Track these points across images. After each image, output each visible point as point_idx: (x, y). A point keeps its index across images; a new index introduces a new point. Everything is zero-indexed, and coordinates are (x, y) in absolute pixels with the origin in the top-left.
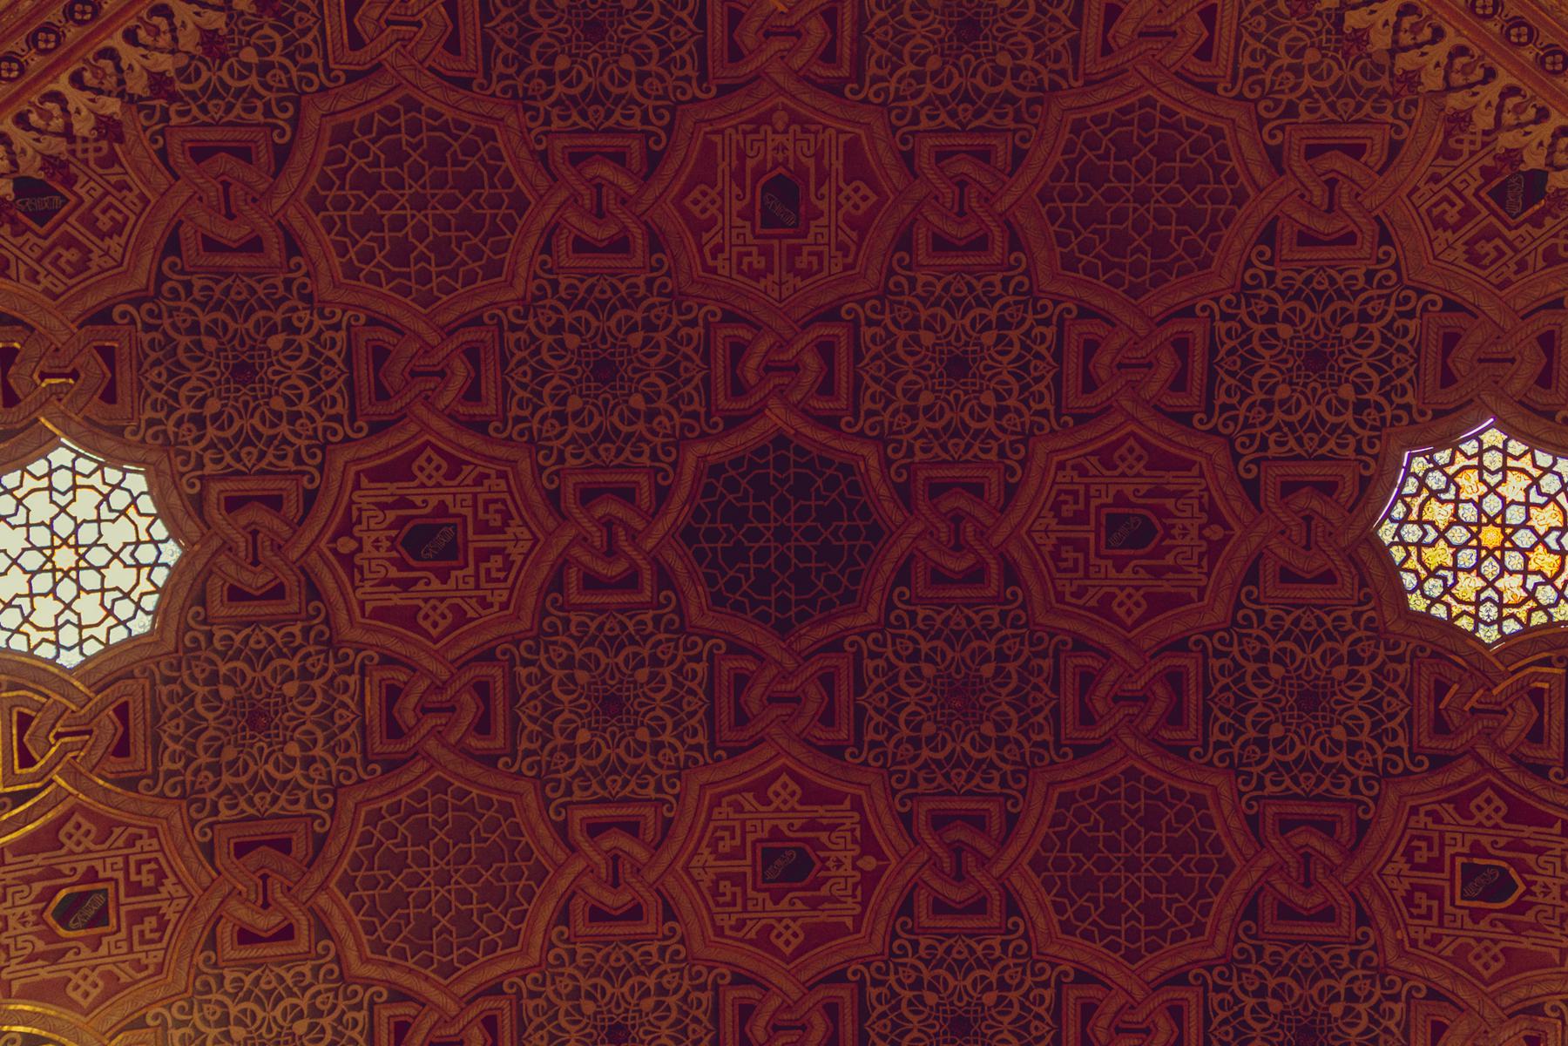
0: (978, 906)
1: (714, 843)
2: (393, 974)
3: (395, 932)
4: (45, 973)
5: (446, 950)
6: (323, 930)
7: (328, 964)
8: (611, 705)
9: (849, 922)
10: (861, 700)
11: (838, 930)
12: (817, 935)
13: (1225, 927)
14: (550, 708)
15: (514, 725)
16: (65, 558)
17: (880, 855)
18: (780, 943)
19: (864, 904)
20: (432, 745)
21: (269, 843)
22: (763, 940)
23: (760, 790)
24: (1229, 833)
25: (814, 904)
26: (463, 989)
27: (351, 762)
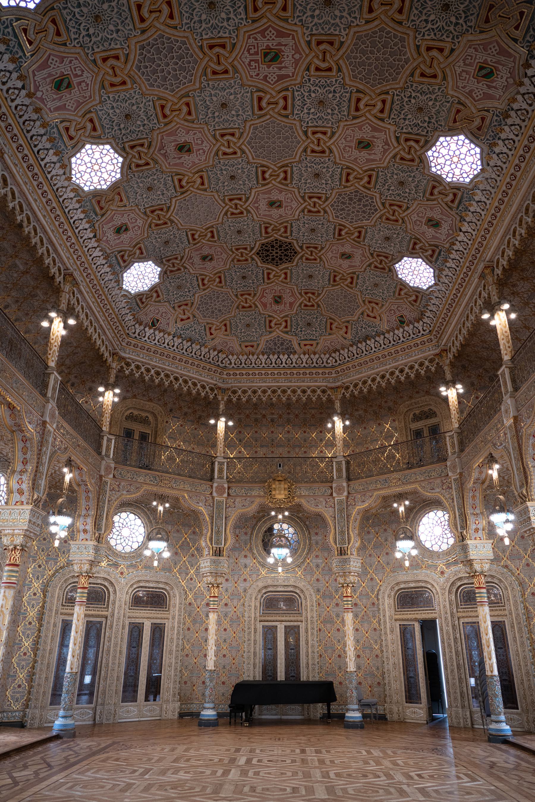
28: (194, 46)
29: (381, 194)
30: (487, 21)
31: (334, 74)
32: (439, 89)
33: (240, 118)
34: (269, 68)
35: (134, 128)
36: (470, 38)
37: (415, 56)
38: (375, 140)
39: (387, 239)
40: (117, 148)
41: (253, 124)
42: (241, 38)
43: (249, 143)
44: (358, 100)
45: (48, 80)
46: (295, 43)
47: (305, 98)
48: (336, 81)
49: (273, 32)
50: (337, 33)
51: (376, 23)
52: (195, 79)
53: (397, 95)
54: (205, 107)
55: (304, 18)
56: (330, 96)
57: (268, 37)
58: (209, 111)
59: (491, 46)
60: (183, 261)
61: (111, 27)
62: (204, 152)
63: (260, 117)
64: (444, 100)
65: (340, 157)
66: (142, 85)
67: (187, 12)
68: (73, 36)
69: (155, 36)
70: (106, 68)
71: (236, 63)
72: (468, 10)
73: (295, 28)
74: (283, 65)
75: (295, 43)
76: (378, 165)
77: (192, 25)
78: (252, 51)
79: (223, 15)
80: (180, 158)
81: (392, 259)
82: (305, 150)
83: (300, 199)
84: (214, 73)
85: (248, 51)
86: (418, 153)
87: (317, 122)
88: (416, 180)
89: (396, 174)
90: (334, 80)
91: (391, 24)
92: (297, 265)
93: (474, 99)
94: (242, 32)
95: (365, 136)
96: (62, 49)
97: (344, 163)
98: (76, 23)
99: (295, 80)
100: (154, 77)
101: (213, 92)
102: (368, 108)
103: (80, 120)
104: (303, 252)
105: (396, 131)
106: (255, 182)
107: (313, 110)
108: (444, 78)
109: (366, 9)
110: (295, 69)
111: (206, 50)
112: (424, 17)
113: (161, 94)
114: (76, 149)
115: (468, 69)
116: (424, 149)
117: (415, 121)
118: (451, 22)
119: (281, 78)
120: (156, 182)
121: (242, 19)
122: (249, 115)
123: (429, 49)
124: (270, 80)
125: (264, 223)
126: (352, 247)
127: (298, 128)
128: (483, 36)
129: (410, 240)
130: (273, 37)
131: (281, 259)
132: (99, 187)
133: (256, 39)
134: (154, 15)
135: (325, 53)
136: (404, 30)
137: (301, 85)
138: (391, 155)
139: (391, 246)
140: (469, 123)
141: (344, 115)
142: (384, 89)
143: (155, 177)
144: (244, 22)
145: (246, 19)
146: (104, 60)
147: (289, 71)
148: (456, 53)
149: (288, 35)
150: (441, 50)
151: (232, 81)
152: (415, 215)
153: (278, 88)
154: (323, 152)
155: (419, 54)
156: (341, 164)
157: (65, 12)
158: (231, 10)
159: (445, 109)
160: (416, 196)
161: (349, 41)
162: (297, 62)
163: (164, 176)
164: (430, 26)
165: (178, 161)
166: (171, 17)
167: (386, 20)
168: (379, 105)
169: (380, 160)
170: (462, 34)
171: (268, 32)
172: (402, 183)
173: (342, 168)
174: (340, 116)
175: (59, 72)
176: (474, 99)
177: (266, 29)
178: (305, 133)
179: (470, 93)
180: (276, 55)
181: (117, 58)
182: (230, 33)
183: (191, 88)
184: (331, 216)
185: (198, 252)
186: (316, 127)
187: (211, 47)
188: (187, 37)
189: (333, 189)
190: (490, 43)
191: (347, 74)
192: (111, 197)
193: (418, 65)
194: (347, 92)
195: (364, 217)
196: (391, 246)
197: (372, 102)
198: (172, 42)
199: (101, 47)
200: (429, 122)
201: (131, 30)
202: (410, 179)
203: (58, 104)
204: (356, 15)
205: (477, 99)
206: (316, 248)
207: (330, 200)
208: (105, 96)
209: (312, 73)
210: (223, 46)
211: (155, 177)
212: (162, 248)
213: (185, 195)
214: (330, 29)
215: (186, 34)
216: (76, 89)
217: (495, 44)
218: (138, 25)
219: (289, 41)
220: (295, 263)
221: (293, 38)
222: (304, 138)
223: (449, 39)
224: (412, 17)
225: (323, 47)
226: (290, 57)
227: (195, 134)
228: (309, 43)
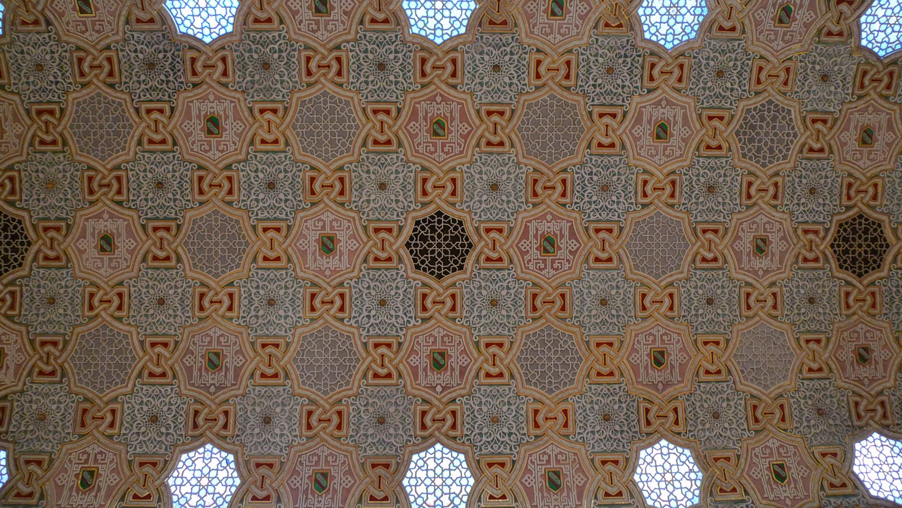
0: (119, 179)
1: (99, 268)
2: (133, 377)
3: (118, 376)
4: (103, 492)
5: (126, 359)
6: (115, 400)
7: (126, 398)
8: (52, 301)
9: (126, 223)
10: (53, 218)
11: (128, 226)
12: (130, 234)
13: (119, 95)
14: (50, 322)
15: (56, 334)
16: (204, 482)
17: (103, 212)
18: (132, 247)
19: (119, 218)
20: (59, 361)
21: (535, 416)
22: (131, 252)
23: (82, 252)
24: (88, 94)
25: (119, 235)
26: (141, 353)
27: (61, 388)
28: (532, 327)
29: (740, 99)
30: (504, 23)
31: (569, 176)
32: (582, 54)
33: (621, 284)
34: (561, 249)
35: (622, 414)
36: (523, 35)
37: (547, 89)
38: (653, 118)
39: (825, 78)
40: (647, 442)
41: (631, 269)
42: (528, 277)
43: (657, 276)
44: (600, 145)
45: (545, 494)
46: (535, 219)
47: (598, 207)
48: (577, 173)
49: (522, 243)
50: (524, 176)
51: (514, 137)
52: (569, 331)
53: (593, 101)
54: (604, 324)
55: (510, 211)
56: (595, 178)
57: (528, 248)
58: (610, 321)
59: (529, 10)
60: (864, 394)
61: (505, 409)
62: (666, 334)
63: (620, 260)
64: (595, 46)
65: (682, 161)
66: (570, 392)
67: (498, 329)
68: (508, 451)
69: (519, 366)
70: (545, 426)
71: (554, 284)
72: (497, 45)
73: (520, 220)
74: (558, 233)
75: (535, 219)
76: (692, 109)
77: (511, 326)
78: (542, 266)
79: (504, 293)
80: (672, 367)
81: (867, 63)
82: (672, 206)
83: (752, 212)
84: (563, 309)
85: (541, 269)
86: (670, 61)
87: (630, 192)
88: (712, 55)
89: (706, 84)
90: (576, 176)
91: (514, 121)
92: (888, 214)
93: (589, 11)
94: (522, 275)
95: (649, 132)
96: (517, 466)
97: (690, 155)
98: (495, 443)
99: (575, 219)
100: (562, 377)
101: (586, 313)
102: (610, 132)
103: (600, 476)
104: (860, 204)
105: (640, 95)
106: (721, 272)
107: (614, 198)
108: (570, 51)
109: (500, 149)
110: (563, 219)
111: (537, 314)
112: (507, 88)
113: (584, 373)
114: (636, 494)
115: (555, 28)
116: (663, 55)
117: (625, 74)
118: (510, 59)
119: (572, 235)
120: (706, 405)
121: (509, 274)
122: (618, 274)
123: (538, 76)
124: (575, 248)
125: (797, 262)
126: (847, 129)
127: (638, 215)
128: (520, 22)
129: (825, 43)
130: (528, 243)
131: (874, 240)
132: (699, 483)
133: (530, 260)
134: (498, 362)
135: (545, 188)
136: (520, 106)
137: (582, 211)
138: (675, 95)
139: (840, 70)
140: (620, 8)
141: (620, 160)
142: (585, 118)
143: (698, 404)
144: (512, 272)
145: (509, 269)
146: (537, 426)
147: (566, 226)
148: (540, 45)
149: (527, 227)
150: (539, 63)
151: (574, 290)
152: (774, 44)
153: (585, 239)
154: (673, 183)
155: (544, 85)
156: (692, 158)
157: (484, 451)
158: (500, 284)
159: (606, 42)
160: (740, 50)
161: (533, 163)
162: (555, 218)
163: (698, 392)
164: (515, 81)
165: (677, 370)
166: (500, 345)
167: (510, 126)
168: (607, 120)
169: (683, 108)
170: (521, 44)
171: (522, 248)
172: (720, 74)
173: (699, 157)
174: (622, 165)
175: (540, 479)
176: (589, 11)
177: (520, 250)
178: (644, 206)
179: (582, 18)
180: (547, 240)
181: (536, 412)
182: (522, 288)
183: (579, 338)
184: (783, 166)
185: (849, 368)
186: (636, 193)
187: (535, 309)
188: (522, 333)
189: (734, 168)
190: (526, 12)
191: (570, 162)
192: (718, 473)
193: (556, 84)
194: (591, 159)
195: (784, 118)
196: (840, 70)
197: (603, 128)
198: (526, 350)
199: (523, 425)
200: (626, 56)
201: (510, 389)
202: (712, 63)
203: (575, 493)
204: (506, 158)
205: (588, 8)
206: (850, 186)
207: (752, 169)
208: (578, 437)
209: (568, 200)
210: (535, 296)
211: (698, 404)
212: (831, 422)
213: (733, 370)
214: (521, 184)
215: (520, 333)
216: (563, 467)
217: (526, 7)
218: (505, 380)
219: (532, 226)
220: (885, 218)
221: (530, 221)
222: (652, 208)
223: (527, 56)
224: (508, 101)
225: (539, 190)
226: (549, 224)
227: (639, 342)
228: (535, 205)
